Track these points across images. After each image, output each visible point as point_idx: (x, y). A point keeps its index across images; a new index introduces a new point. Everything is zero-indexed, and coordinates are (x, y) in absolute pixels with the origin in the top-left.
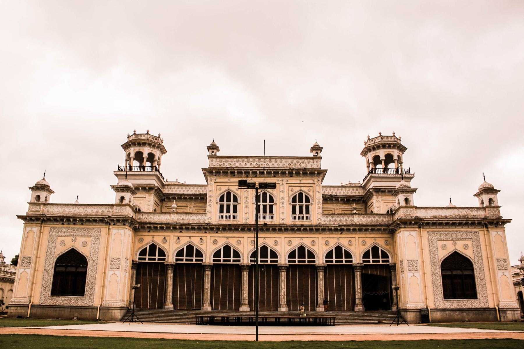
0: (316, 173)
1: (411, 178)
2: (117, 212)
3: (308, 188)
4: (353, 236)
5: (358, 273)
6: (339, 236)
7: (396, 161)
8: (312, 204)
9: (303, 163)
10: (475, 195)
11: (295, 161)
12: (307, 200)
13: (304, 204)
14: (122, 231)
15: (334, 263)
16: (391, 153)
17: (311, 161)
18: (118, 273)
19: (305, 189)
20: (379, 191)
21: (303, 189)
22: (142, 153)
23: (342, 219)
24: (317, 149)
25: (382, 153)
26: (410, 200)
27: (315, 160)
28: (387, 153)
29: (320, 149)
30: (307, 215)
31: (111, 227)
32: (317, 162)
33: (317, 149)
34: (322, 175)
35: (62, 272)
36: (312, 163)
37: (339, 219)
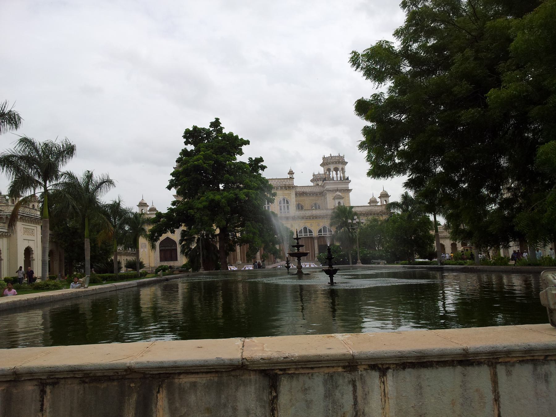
1: (349, 182)
12: (287, 202)
13: (286, 205)
19: (286, 197)
24: (291, 173)
33: (291, 173)
35: (164, 250)
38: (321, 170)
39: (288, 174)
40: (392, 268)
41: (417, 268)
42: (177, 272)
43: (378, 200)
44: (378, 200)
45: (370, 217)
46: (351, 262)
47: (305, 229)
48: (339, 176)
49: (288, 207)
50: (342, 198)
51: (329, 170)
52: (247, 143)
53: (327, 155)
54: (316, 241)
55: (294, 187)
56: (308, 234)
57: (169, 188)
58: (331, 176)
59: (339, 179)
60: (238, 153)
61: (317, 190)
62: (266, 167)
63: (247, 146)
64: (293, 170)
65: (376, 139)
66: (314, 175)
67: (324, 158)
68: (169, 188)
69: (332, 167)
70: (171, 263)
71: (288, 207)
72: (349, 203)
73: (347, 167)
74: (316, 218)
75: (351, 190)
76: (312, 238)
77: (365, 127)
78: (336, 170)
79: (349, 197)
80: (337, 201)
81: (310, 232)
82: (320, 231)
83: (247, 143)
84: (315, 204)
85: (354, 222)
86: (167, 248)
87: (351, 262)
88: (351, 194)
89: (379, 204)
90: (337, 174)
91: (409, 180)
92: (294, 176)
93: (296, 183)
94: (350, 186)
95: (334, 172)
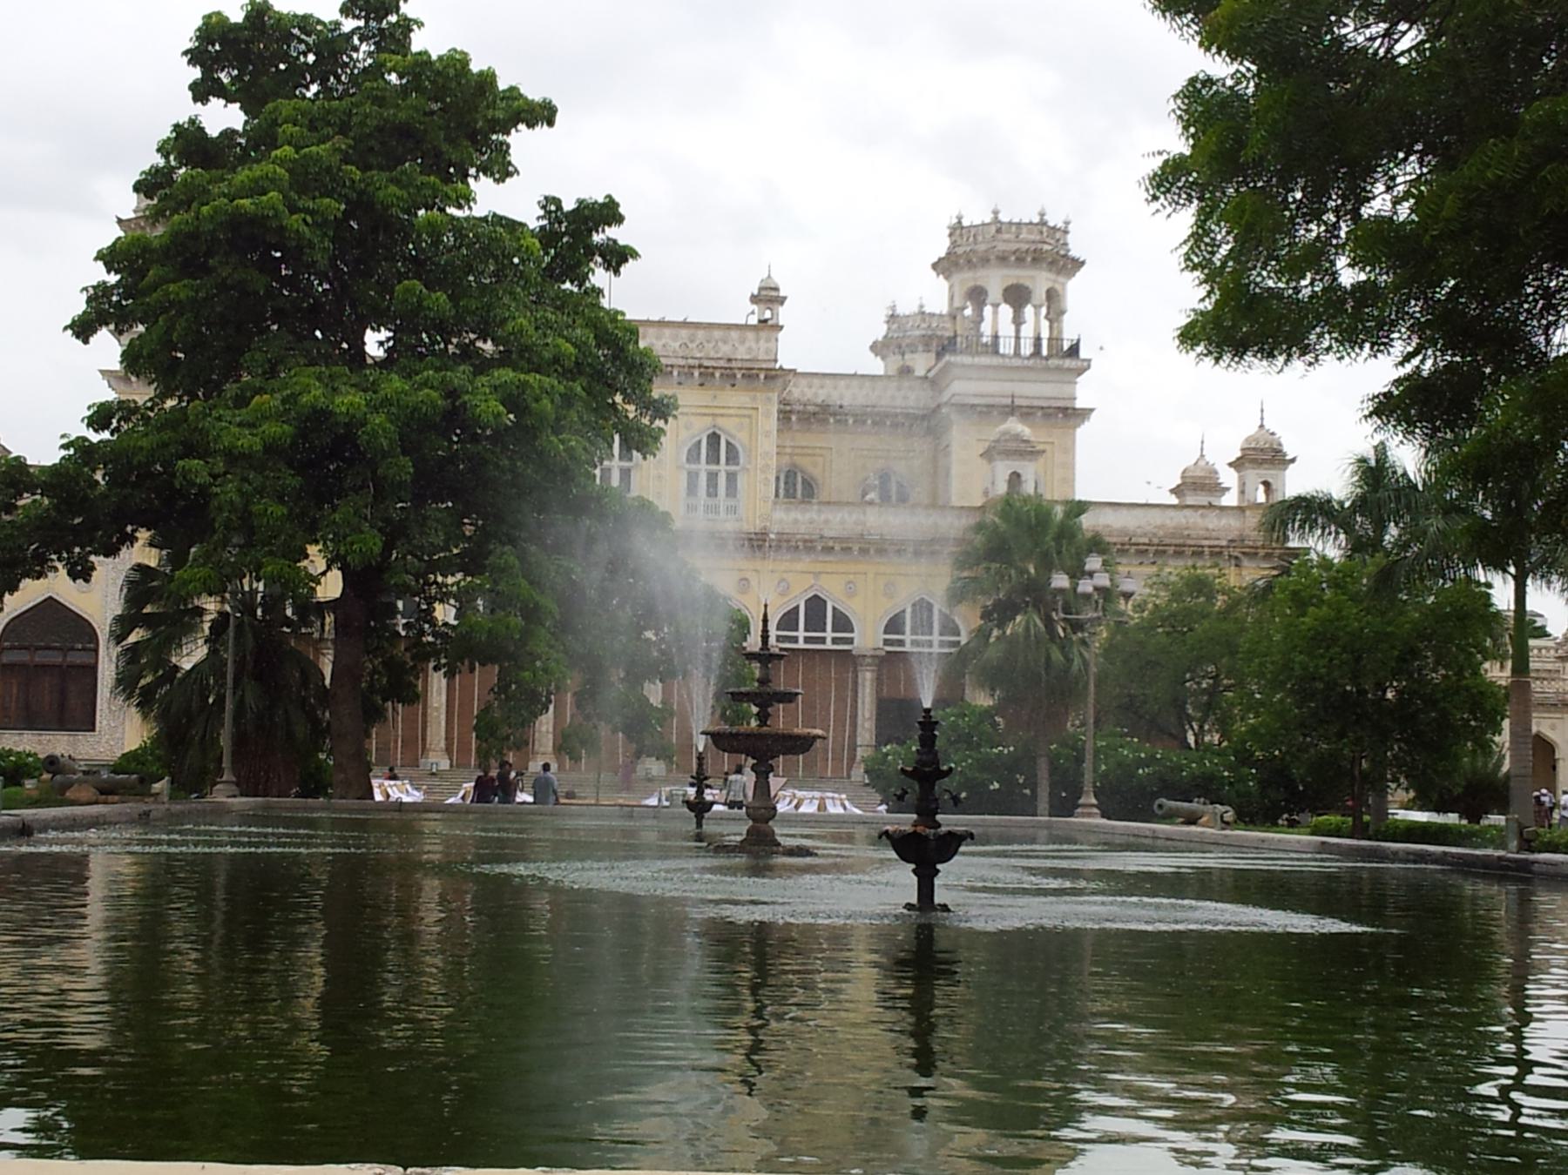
0: (762, 376)
1: (1080, 371)
3: (737, 420)
4: (861, 567)
5: (868, 675)
6: (819, 567)
8: (744, 469)
9: (725, 342)
10: (1230, 465)
11: (701, 334)
12: (733, 456)
13: (723, 467)
15: (801, 645)
17: (750, 335)
21: (720, 421)
23: (830, 517)
24: (768, 296)
27: (763, 334)
29: (782, 301)
30: (731, 502)
32: (768, 340)
33: (768, 296)
34: (779, 382)
36: (754, 345)
37: (823, 517)
38: (936, 295)
39: (755, 299)
40: (1258, 847)
41: (1395, 857)
42: (88, 793)
43: (1229, 478)
44: (1229, 478)
45: (1174, 570)
46: (1043, 803)
47: (816, 606)
48: (1027, 331)
49: (732, 478)
50: (1028, 451)
51: (978, 296)
52: (543, 114)
53: (976, 215)
54: (867, 678)
55: (774, 376)
56: (829, 634)
57: (83, 329)
58: (986, 328)
59: (1027, 349)
60: (485, 169)
61: (912, 398)
62: (634, 254)
63: (542, 130)
64: (778, 279)
65: (1248, 155)
66: (893, 318)
67: (957, 229)
68: (83, 329)
69: (995, 281)
70: (58, 744)
71: (732, 478)
72: (1069, 481)
73: (1075, 289)
74: (881, 551)
75: (1085, 414)
76: (847, 660)
77: (1193, 81)
78: (1017, 297)
79: (1069, 450)
80: (1003, 469)
81: (843, 623)
82: (894, 625)
83: (543, 114)
84: (884, 478)
85: (1085, 586)
86: (40, 657)
87: (1043, 803)
88: (1083, 433)
89: (1230, 499)
90: (1018, 321)
91: (1398, 382)
92: (784, 314)
93: (792, 352)
94: (1085, 393)
95: (1006, 311)
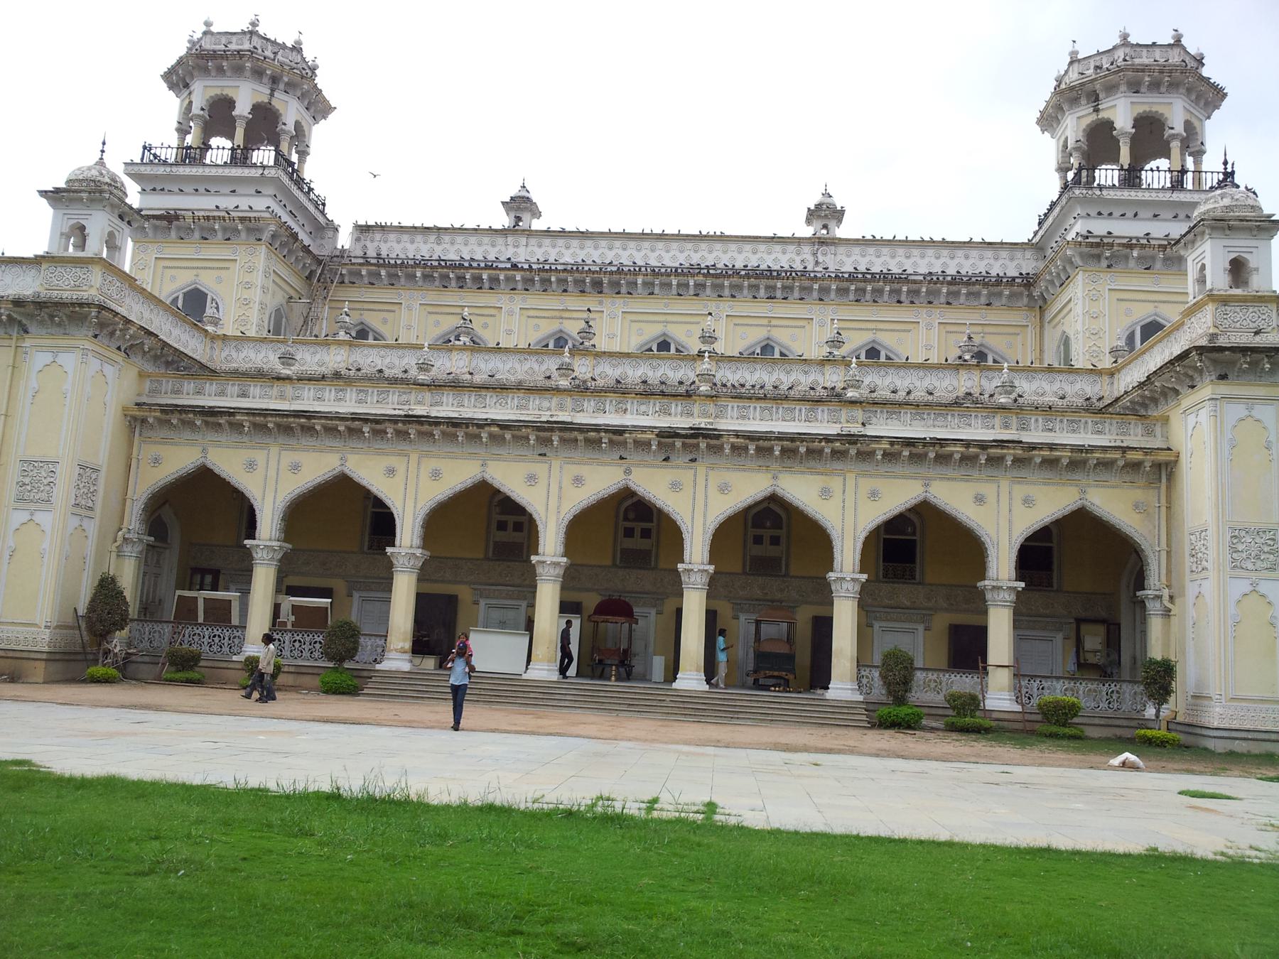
2: (65, 285)
7: (1175, 146)
14: (69, 360)
16: (1161, 109)
18: (44, 519)
20: (1099, 252)
22: (229, 103)
25: (1122, 113)
26: (1252, 264)
28: (1140, 109)
31: (28, 343)
